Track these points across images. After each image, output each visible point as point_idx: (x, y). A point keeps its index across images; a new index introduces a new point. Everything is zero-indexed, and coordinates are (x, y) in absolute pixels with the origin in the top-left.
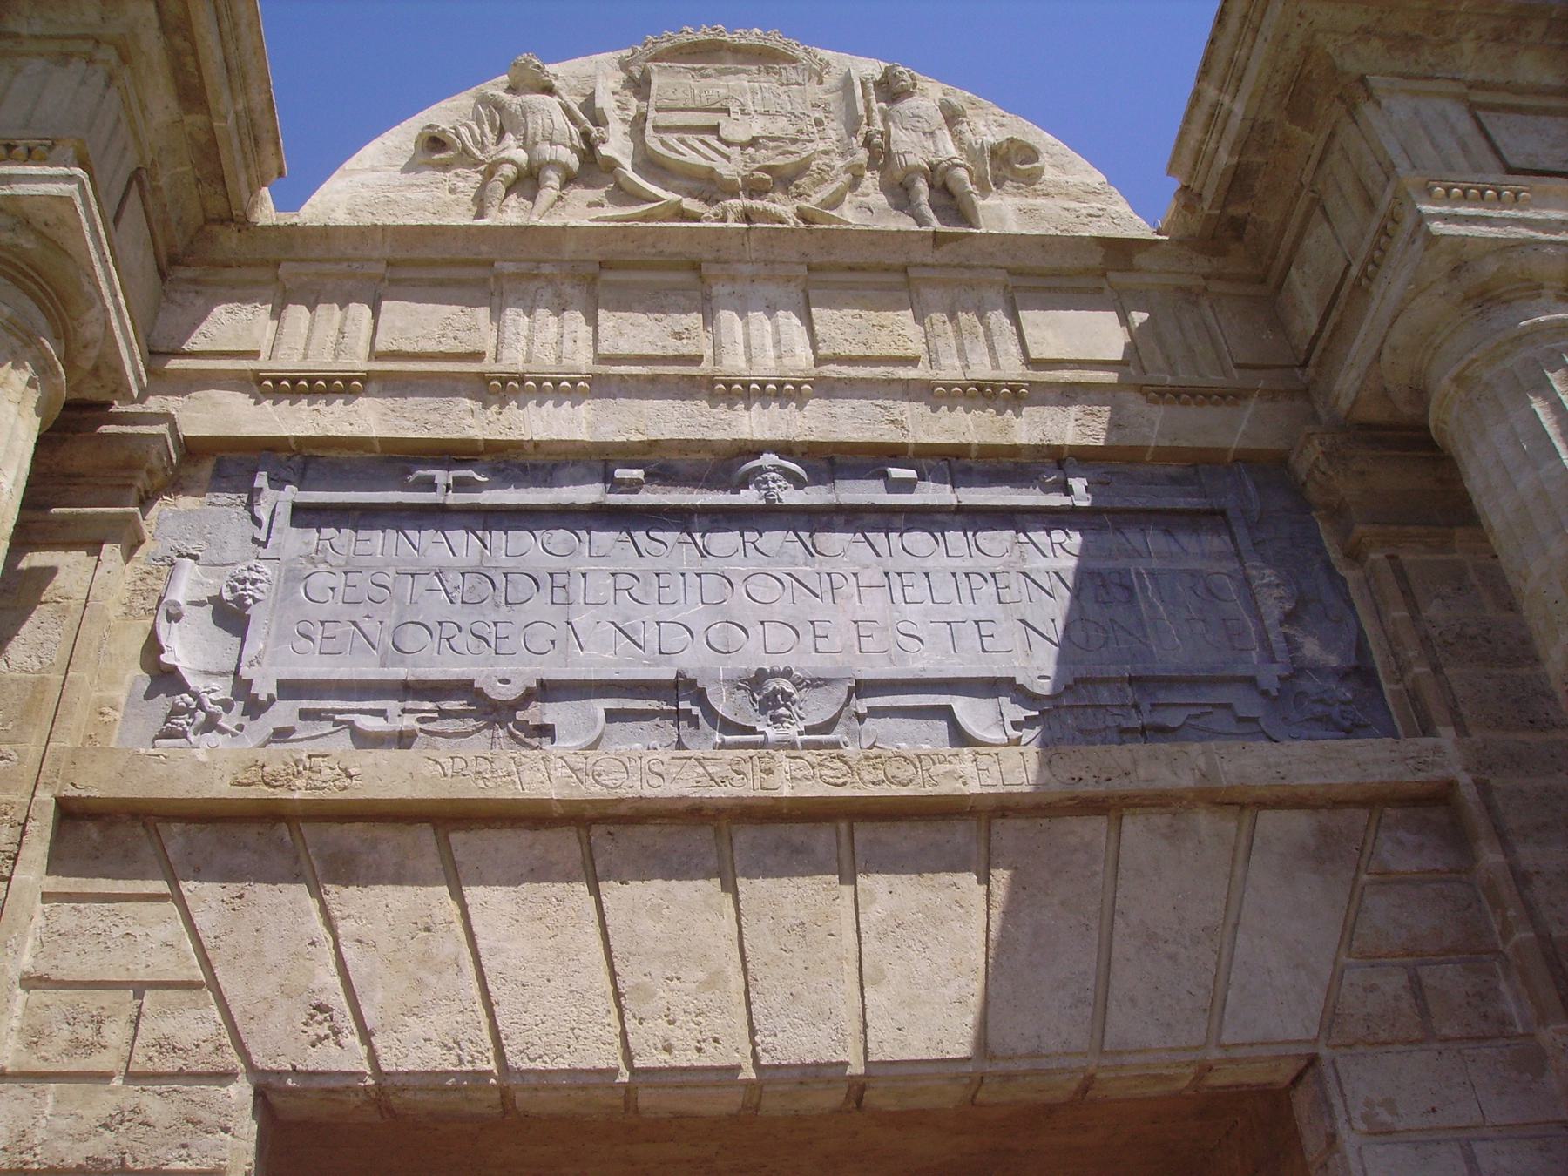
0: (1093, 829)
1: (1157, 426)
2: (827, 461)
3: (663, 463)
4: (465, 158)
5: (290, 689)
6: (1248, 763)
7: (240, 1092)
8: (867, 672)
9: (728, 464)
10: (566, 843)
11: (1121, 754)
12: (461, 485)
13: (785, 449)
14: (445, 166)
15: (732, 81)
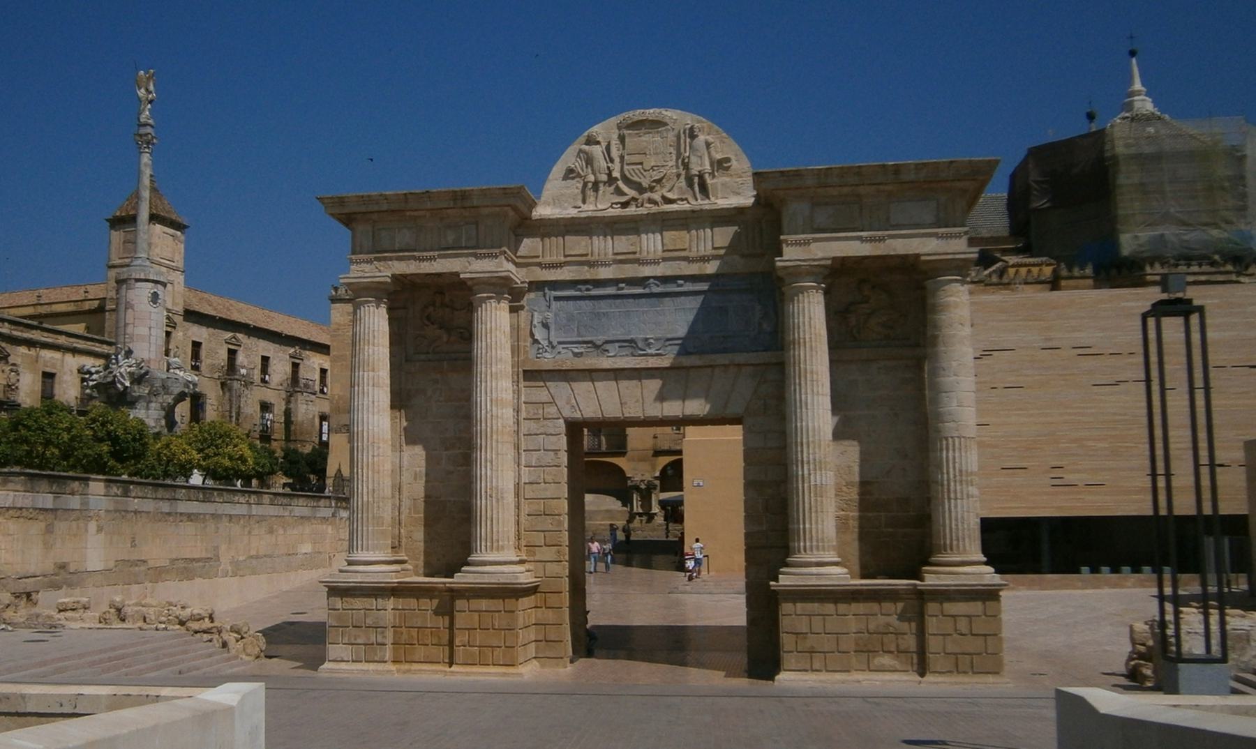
0: (709, 370)
1: (739, 264)
2: (665, 280)
3: (632, 282)
4: (579, 176)
5: (560, 343)
6: (741, 358)
7: (562, 421)
8: (669, 336)
9: (642, 282)
10: (611, 374)
11: (713, 357)
12: (588, 290)
13: (655, 278)
14: (573, 178)
15: (646, 138)
